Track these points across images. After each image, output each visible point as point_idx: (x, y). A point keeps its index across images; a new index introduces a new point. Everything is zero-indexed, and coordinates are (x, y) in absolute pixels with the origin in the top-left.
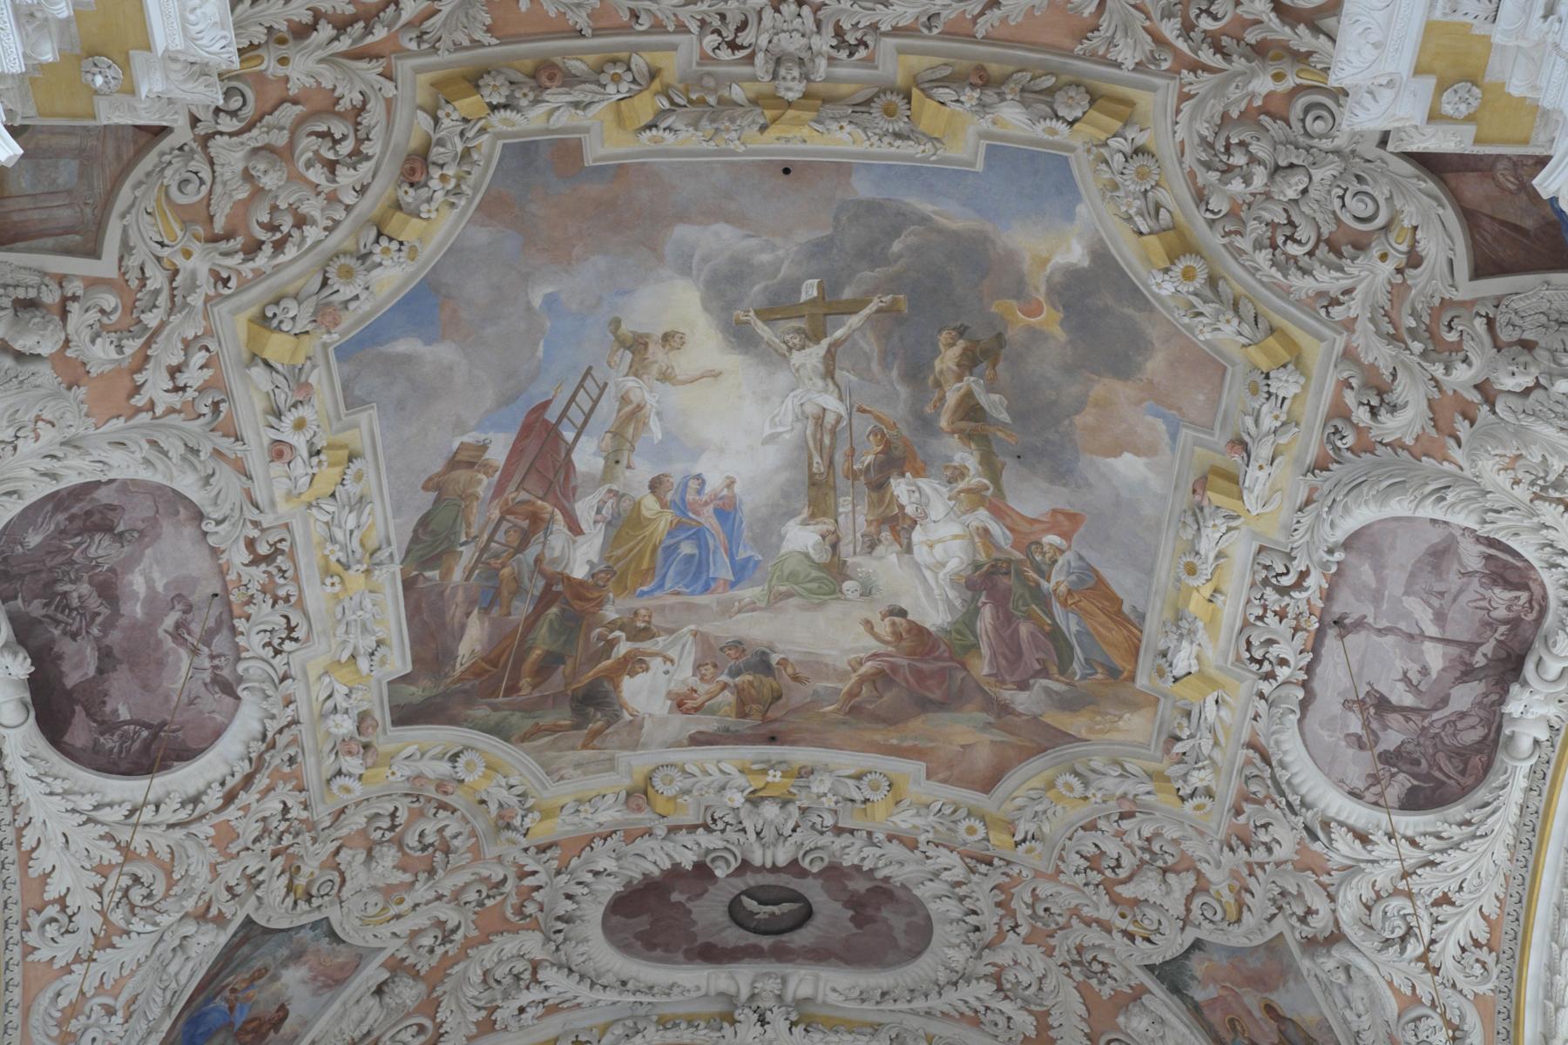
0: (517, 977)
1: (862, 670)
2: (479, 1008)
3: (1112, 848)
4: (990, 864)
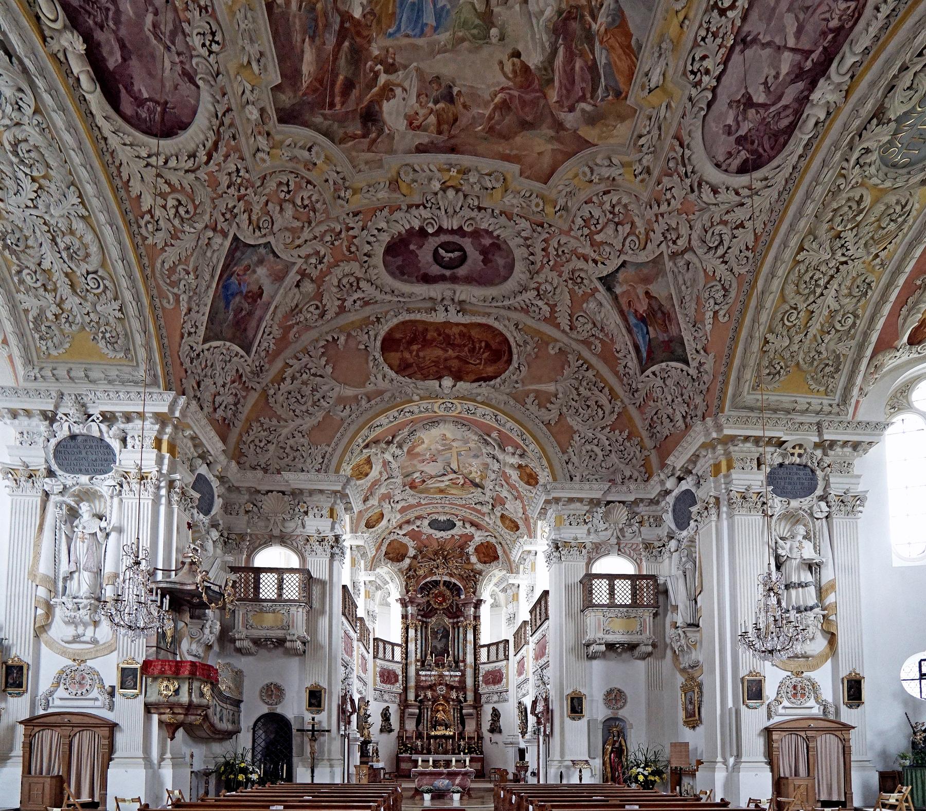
0: (351, 285)
1: (496, 100)
2: (339, 299)
3: (597, 213)
4: (543, 227)
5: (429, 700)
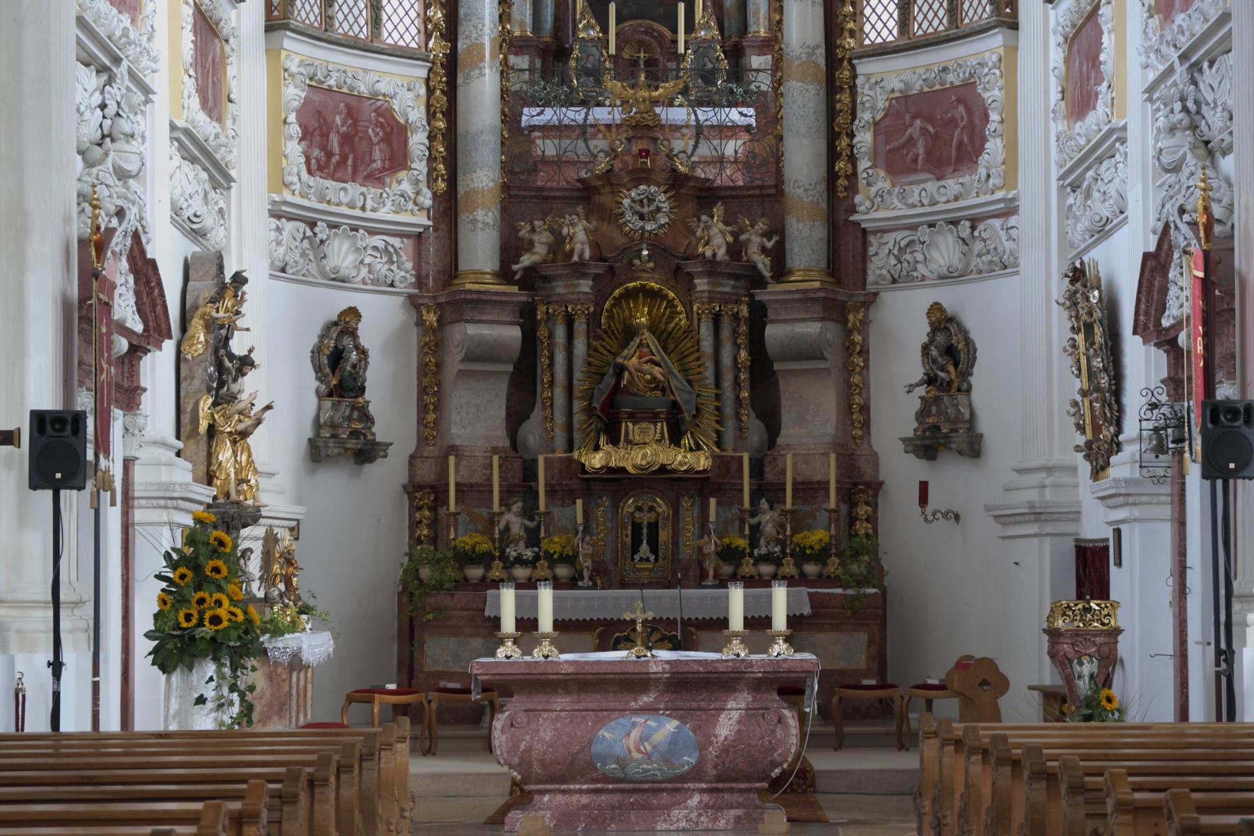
5: (579, 269)
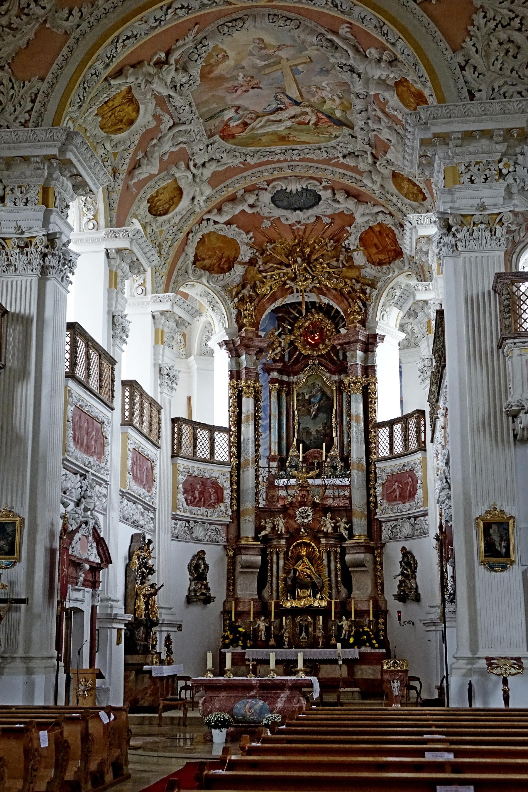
5: (280, 536)
